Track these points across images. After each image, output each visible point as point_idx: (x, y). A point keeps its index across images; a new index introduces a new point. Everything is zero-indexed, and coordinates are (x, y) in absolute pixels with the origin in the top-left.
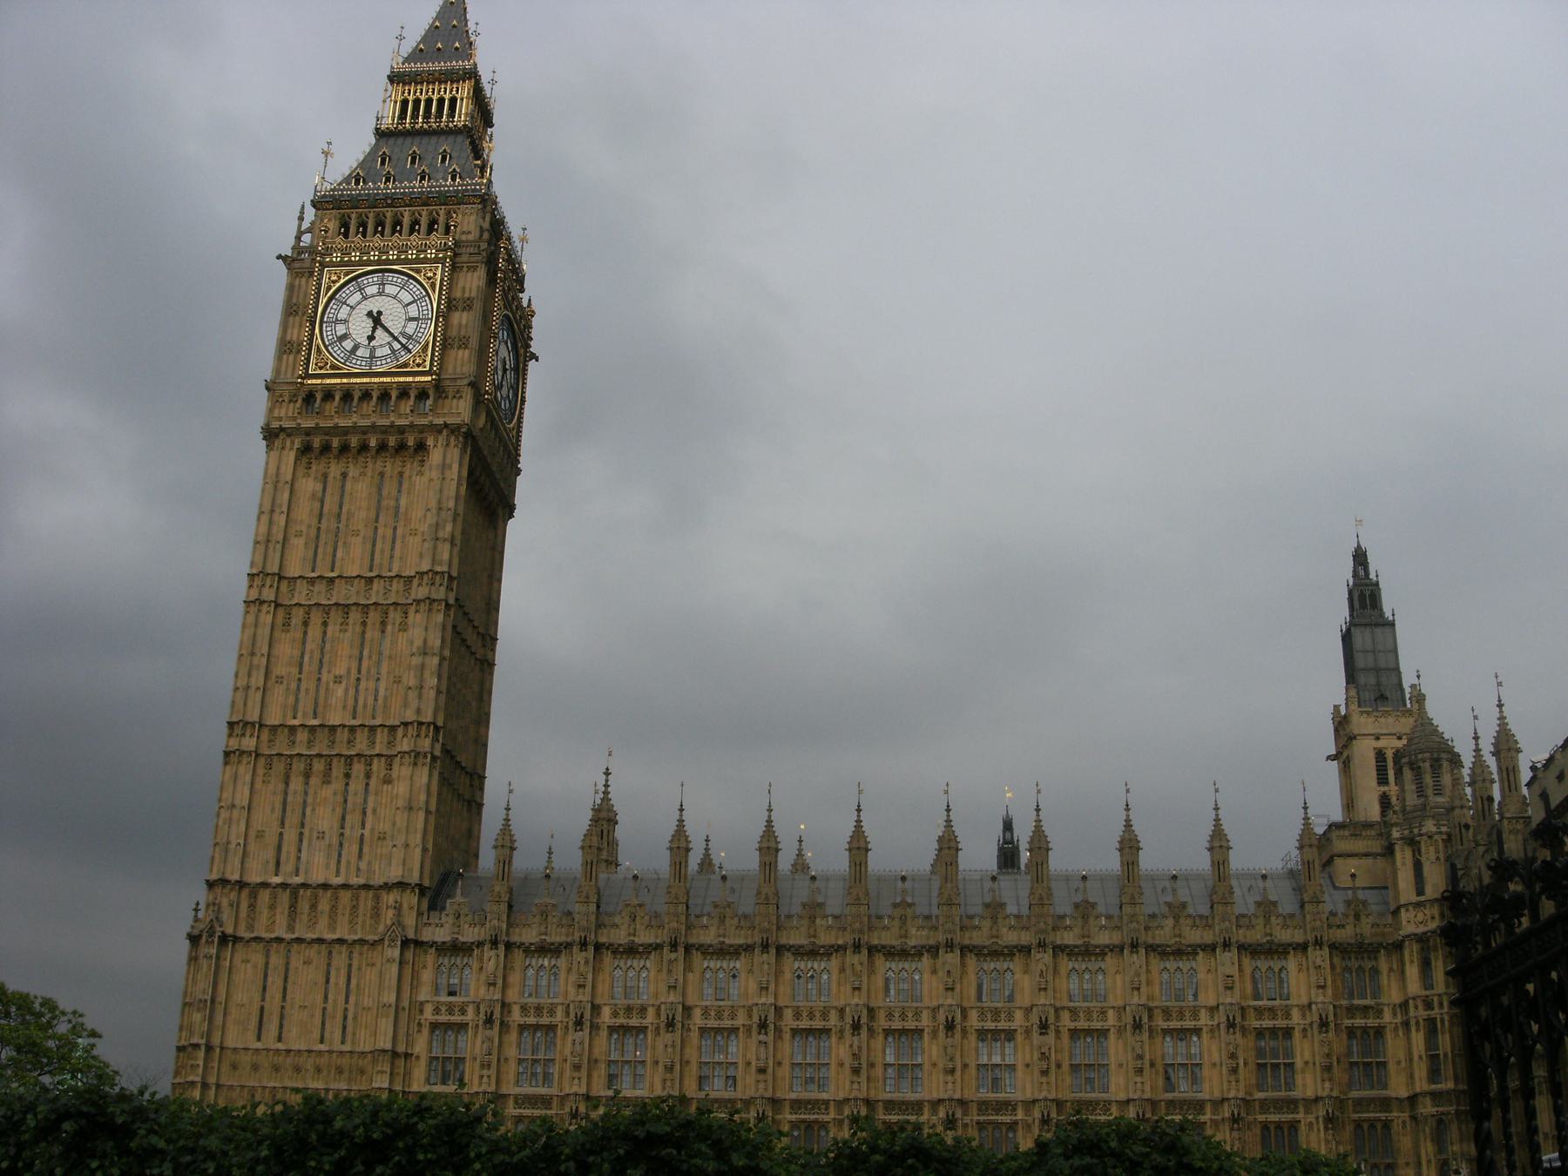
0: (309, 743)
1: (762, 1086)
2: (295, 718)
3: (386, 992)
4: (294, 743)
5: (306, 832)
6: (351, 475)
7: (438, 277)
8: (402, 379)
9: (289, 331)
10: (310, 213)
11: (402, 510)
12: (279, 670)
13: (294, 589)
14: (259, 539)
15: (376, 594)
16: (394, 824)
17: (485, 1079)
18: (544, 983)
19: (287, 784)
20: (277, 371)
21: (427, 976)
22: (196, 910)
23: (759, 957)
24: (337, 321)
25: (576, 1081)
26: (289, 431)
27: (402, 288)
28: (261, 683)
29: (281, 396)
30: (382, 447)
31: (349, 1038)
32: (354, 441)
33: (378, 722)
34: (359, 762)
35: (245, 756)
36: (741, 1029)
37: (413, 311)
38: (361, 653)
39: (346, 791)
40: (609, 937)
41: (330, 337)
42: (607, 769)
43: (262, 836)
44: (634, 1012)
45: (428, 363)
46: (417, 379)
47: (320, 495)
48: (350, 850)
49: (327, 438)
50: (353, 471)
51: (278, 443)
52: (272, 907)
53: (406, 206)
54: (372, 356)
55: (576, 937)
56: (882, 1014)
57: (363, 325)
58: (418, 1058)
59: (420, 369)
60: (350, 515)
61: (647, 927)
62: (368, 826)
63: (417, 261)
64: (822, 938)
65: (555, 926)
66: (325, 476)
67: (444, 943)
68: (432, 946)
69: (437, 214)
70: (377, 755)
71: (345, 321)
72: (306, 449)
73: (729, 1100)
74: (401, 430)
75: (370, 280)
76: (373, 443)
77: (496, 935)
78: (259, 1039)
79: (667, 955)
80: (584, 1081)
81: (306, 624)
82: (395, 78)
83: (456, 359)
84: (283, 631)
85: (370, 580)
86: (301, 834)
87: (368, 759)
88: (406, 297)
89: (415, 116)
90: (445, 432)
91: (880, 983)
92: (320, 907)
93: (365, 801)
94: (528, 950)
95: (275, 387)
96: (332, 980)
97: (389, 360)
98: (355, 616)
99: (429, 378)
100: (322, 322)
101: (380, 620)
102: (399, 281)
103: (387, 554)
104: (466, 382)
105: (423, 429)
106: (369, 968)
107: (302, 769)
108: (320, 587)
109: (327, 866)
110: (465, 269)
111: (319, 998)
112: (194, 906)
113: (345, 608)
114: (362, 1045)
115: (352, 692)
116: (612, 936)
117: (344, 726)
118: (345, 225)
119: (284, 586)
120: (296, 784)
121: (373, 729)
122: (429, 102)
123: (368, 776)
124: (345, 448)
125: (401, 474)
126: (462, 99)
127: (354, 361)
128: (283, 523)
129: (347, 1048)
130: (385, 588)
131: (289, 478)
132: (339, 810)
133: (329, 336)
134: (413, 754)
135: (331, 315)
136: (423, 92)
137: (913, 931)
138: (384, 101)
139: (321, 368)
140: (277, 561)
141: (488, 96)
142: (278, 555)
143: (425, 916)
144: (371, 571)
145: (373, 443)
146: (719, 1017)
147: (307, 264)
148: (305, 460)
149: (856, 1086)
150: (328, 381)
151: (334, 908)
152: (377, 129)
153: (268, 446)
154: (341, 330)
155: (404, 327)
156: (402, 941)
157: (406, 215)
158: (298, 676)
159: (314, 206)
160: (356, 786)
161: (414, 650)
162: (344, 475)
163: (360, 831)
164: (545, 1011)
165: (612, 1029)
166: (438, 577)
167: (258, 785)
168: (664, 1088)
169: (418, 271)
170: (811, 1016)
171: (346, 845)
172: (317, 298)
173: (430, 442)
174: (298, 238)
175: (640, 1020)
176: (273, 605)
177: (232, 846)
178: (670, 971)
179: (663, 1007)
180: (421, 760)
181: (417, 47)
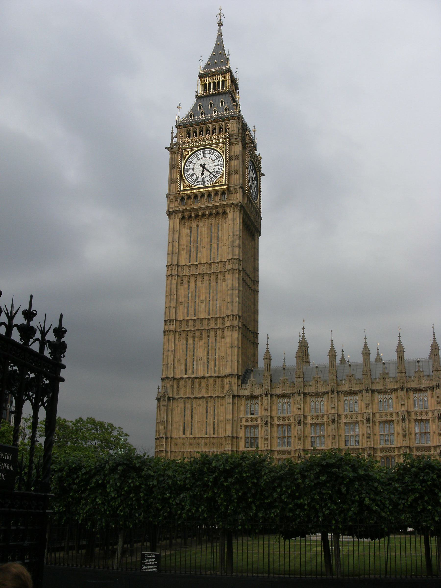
0: (194, 325)
1: (369, 443)
2: (188, 317)
3: (228, 414)
4: (188, 326)
5: (195, 358)
6: (200, 225)
7: (225, 148)
8: (215, 188)
9: (173, 175)
11: (220, 237)
12: (181, 299)
14: (169, 252)
15: (213, 269)
16: (227, 353)
17: (266, 445)
18: (285, 408)
19: (187, 341)
20: (170, 190)
21: (242, 408)
22: (158, 389)
23: (365, 395)
25: (299, 444)
26: (176, 212)
27: (212, 154)
28: (175, 306)
30: (210, 214)
31: (216, 432)
32: (200, 213)
33: (218, 316)
34: (212, 331)
35: (171, 332)
36: (360, 422)
37: (217, 162)
38: (210, 291)
39: (208, 342)
40: (308, 390)
41: (188, 176)
43: (180, 361)
44: (320, 418)
45: (224, 181)
46: (221, 187)
48: (212, 363)
49: (190, 213)
50: (201, 224)
51: (172, 217)
52: (185, 386)
54: (203, 181)
55: (296, 391)
56: (413, 414)
57: (199, 169)
58: (241, 438)
59: (221, 184)
60: (201, 241)
61: (322, 385)
62: (217, 354)
63: (216, 143)
64: (389, 386)
65: (288, 387)
66: (191, 227)
67: (248, 396)
68: (243, 397)
69: (222, 125)
70: (218, 328)
71: (192, 169)
72: (183, 218)
73: (357, 449)
74: (217, 207)
75: (200, 153)
77: (267, 392)
78: (184, 434)
79: (330, 395)
80: (302, 444)
81: (189, 282)
82: (201, 76)
85: (210, 264)
86: (193, 359)
87: (215, 330)
88: (213, 157)
89: (210, 89)
90: (233, 206)
91: (412, 402)
92: (202, 385)
93: (216, 345)
94: (279, 397)
96: (208, 412)
97: (210, 182)
98: (206, 278)
99: (225, 187)
101: (215, 278)
102: (210, 152)
103: (216, 254)
104: (239, 187)
105: (224, 206)
106: (221, 406)
108: (193, 268)
109: (204, 370)
110: (234, 144)
111: (204, 418)
112: (158, 388)
113: (203, 275)
114: (221, 434)
115: (207, 305)
116: (309, 390)
118: (189, 133)
119: (180, 269)
120: (190, 341)
121: (216, 319)
122: (214, 83)
123: (216, 336)
124: (197, 216)
125: (218, 224)
126: (226, 81)
127: (197, 183)
128: (177, 246)
129: (215, 436)
131: (178, 229)
132: (206, 349)
133: (187, 175)
134: (231, 327)
135: (187, 167)
136: (211, 80)
137: (423, 381)
138: (198, 85)
139: (185, 187)
141: (236, 78)
142: (176, 258)
143: (240, 386)
144: (210, 260)
146: (351, 418)
147: (176, 149)
148: (183, 222)
149: (404, 442)
150: (188, 192)
151: (207, 385)
152: (196, 96)
154: (191, 172)
155: (214, 168)
156: (233, 396)
157: (210, 126)
158: (187, 302)
159: (177, 127)
160: (212, 340)
161: (229, 288)
162: (198, 226)
163: (215, 357)
164: (286, 419)
165: (311, 424)
166: (235, 261)
167: (177, 342)
168: (332, 446)
169: (217, 147)
170: (386, 416)
171: (210, 362)
173: (228, 211)
174: (172, 140)
175: (322, 421)
176: (176, 276)
177: (169, 365)
178: (332, 402)
179: (330, 415)
180: (234, 329)
181: (207, 63)
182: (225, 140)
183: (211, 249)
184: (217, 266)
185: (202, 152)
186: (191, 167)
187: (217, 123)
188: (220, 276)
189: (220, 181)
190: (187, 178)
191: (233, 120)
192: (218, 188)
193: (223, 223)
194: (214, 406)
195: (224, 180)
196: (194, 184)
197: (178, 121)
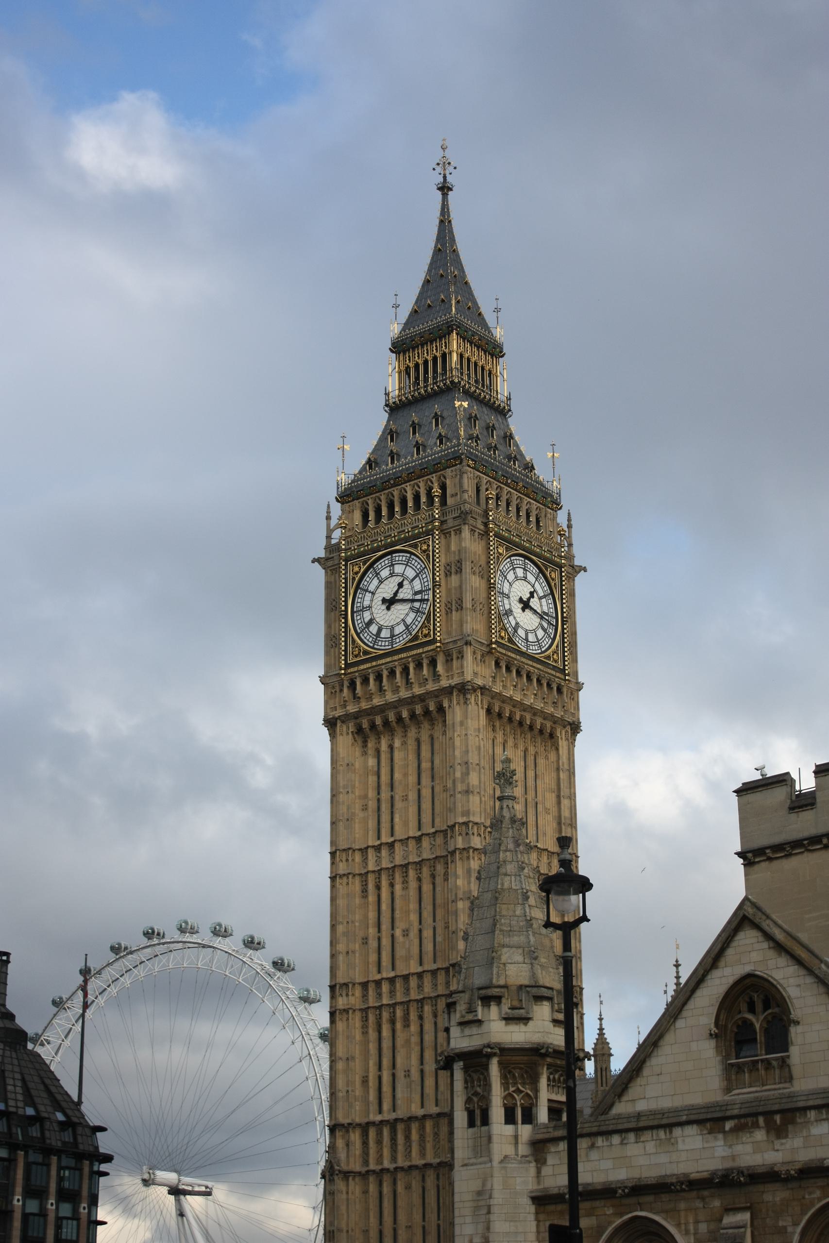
0: (390, 993)
7: (431, 548)
10: (337, 509)
11: (436, 769)
20: (327, 666)
24: (363, 609)
27: (407, 565)
30: (413, 716)
32: (392, 717)
42: (677, 961)
46: (426, 649)
47: (376, 769)
49: (371, 717)
52: (379, 1142)
53: (406, 482)
54: (392, 636)
66: (378, 752)
71: (370, 607)
72: (359, 730)
74: (422, 698)
75: (383, 564)
76: (405, 714)
81: (378, 887)
82: (399, 347)
84: (363, 897)
85: (418, 839)
88: (410, 573)
95: (327, 681)
97: (405, 636)
98: (412, 873)
100: (353, 612)
104: (463, 642)
107: (388, 1017)
110: (453, 533)
117: (413, 974)
120: (386, 1032)
122: (426, 362)
124: (386, 723)
125: (432, 738)
126: (450, 353)
130: (431, 844)
133: (359, 625)
135: (359, 604)
139: (356, 656)
145: (405, 714)
147: (336, 562)
150: (362, 667)
151: (422, 1138)
153: (330, 734)
154: (367, 616)
159: (338, 501)
162: (391, 747)
169: (415, 546)
172: (346, 592)
173: (446, 704)
174: (329, 537)
182: (430, 527)
184: (433, 843)
185: (386, 562)
186: (366, 603)
187: (421, 480)
188: (440, 868)
189: (424, 633)
190: (359, 631)
191: (453, 466)
192: (420, 651)
194: (438, 1186)
196: (374, 644)
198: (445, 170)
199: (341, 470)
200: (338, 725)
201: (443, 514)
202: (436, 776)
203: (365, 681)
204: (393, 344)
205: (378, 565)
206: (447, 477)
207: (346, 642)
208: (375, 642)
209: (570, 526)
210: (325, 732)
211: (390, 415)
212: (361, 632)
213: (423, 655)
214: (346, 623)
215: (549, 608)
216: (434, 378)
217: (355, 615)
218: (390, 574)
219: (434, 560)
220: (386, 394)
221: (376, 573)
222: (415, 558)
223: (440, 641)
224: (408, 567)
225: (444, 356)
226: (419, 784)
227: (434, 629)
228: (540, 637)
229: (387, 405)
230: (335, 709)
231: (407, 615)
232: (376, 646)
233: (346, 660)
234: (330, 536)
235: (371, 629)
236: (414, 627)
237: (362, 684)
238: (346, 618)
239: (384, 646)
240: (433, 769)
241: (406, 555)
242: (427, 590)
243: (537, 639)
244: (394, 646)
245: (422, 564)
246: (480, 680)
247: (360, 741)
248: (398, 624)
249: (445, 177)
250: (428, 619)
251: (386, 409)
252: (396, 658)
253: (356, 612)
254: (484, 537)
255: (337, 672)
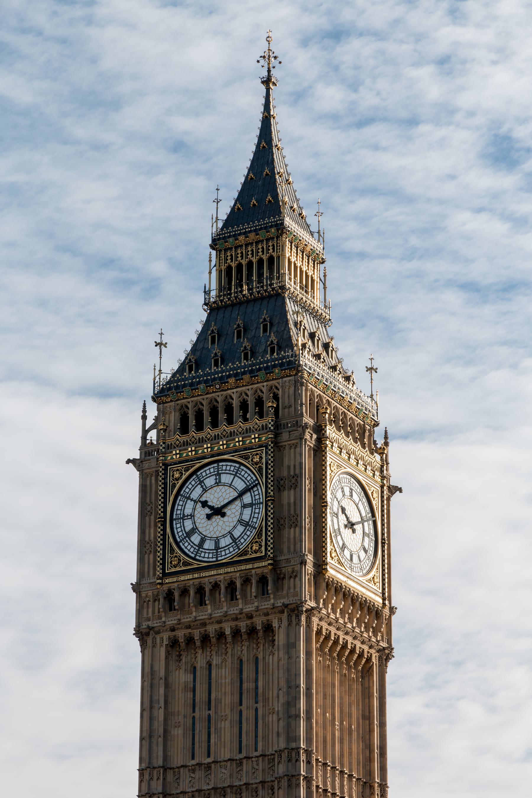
6: (214, 663)
7: (264, 460)
8: (243, 567)
11: (260, 690)
13: (179, 778)
20: (141, 574)
24: (184, 518)
26: (156, 629)
27: (235, 475)
29: (147, 596)
30: (236, 633)
45: (263, 549)
46: (256, 565)
49: (189, 631)
54: (217, 547)
59: (258, 555)
60: (218, 701)
72: (174, 643)
74: (250, 617)
76: (228, 632)
83: (289, 538)
85: (240, 763)
102: (232, 468)
103: (252, 735)
110: (287, 448)
122: (250, 264)
124: (205, 639)
128: (161, 718)
131: (162, 673)
138: (210, 273)
139: (175, 566)
140: (161, 754)
142: (161, 748)
145: (228, 632)
148: (175, 654)
150: (182, 578)
153: (141, 646)
154: (188, 525)
155: (241, 514)
159: (154, 399)
162: (210, 665)
172: (165, 498)
173: (275, 624)
174: (144, 438)
183: (241, 723)
186: (188, 511)
189: (254, 548)
190: (179, 540)
191: (287, 376)
193: (268, 653)
195: (263, 544)
196: (196, 555)
197: (157, 379)
198: (269, 64)
199: (158, 369)
200: (151, 637)
201: (277, 426)
202: (260, 698)
203: (185, 592)
204: (214, 240)
205: (202, 473)
206: (279, 387)
207: (164, 550)
208: (197, 552)
209: (386, 444)
210: (136, 642)
211: (209, 315)
212: (181, 541)
213: (253, 571)
214: (164, 530)
215: (369, 529)
216: (260, 281)
217: (174, 522)
218: (216, 483)
219: (267, 472)
220: (205, 292)
221: (199, 480)
222: (245, 469)
223: (273, 559)
224: (236, 478)
225: (271, 260)
226: (241, 704)
227: (266, 544)
228: (362, 559)
229: (205, 304)
230: (148, 619)
231: (235, 527)
232: (197, 557)
233: (163, 569)
234: (146, 437)
235: (192, 539)
236: (242, 541)
237: (180, 595)
238: (164, 524)
239: (207, 557)
240: (257, 688)
241: (234, 464)
242: (258, 504)
243: (360, 560)
244: (219, 559)
245: (252, 476)
246: (313, 603)
247: (175, 654)
248: (224, 536)
249: (269, 71)
250: (259, 534)
251: (206, 307)
252: (222, 571)
253: (176, 519)
254: (317, 453)
255: (152, 581)
